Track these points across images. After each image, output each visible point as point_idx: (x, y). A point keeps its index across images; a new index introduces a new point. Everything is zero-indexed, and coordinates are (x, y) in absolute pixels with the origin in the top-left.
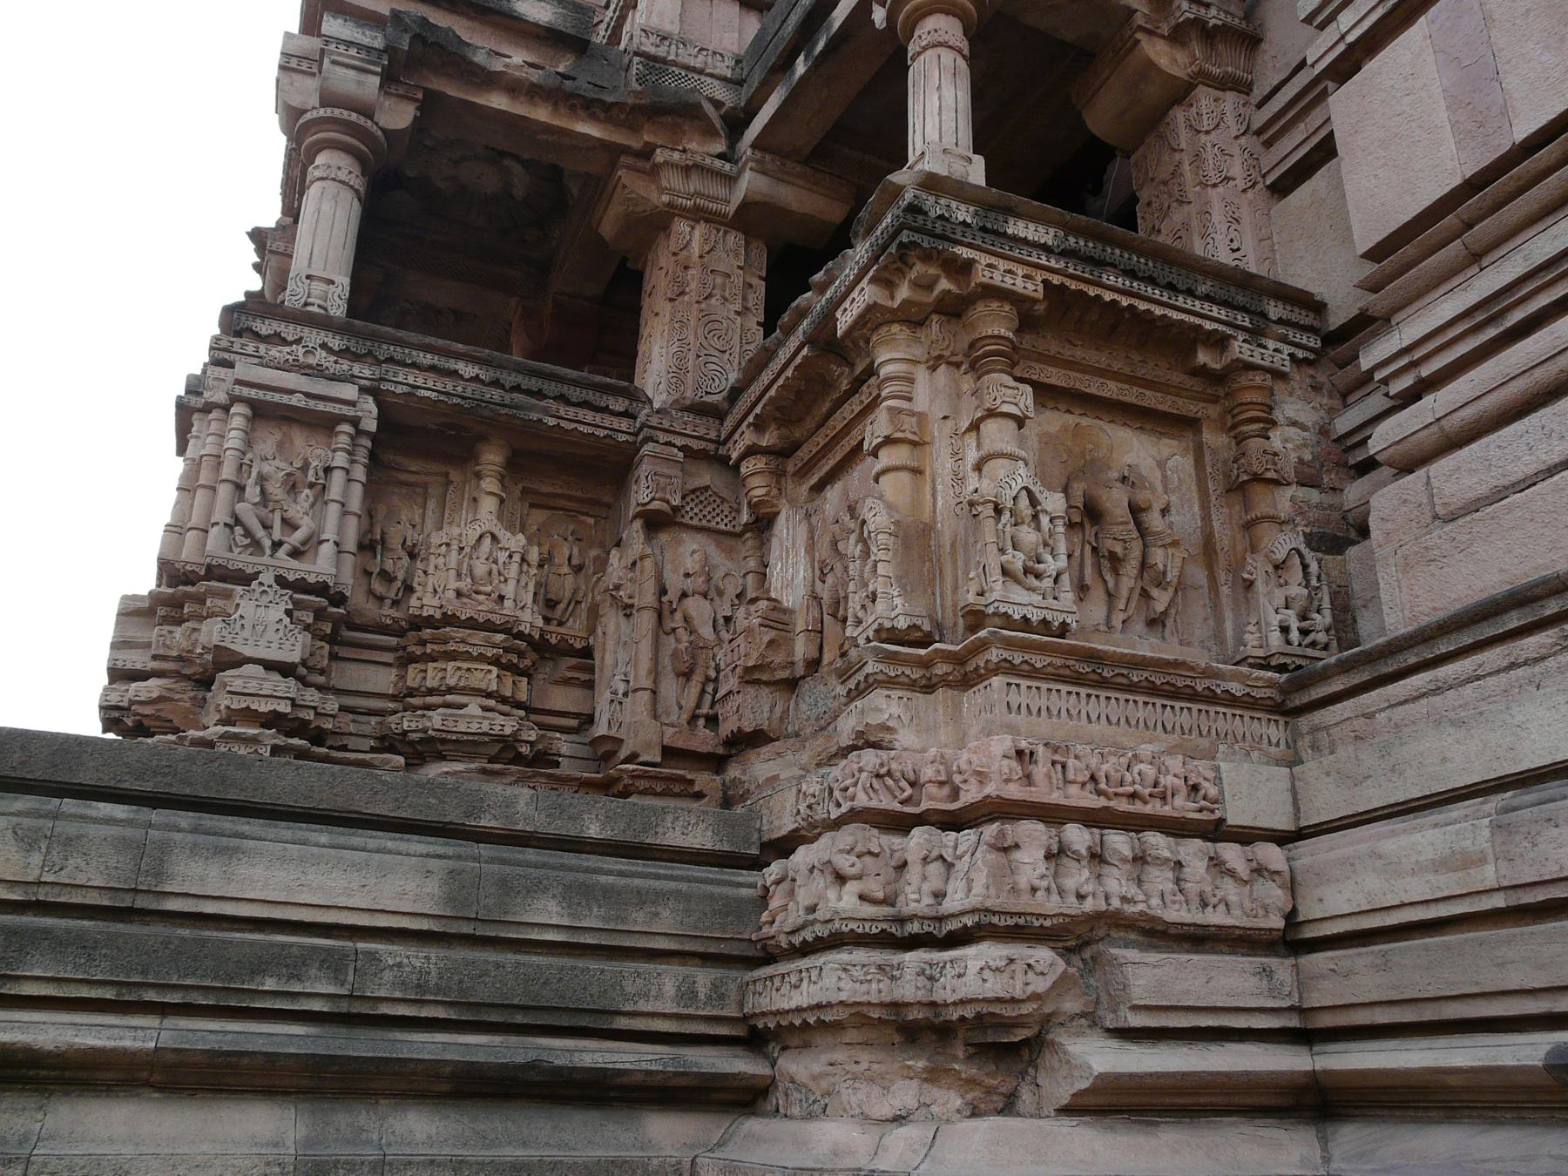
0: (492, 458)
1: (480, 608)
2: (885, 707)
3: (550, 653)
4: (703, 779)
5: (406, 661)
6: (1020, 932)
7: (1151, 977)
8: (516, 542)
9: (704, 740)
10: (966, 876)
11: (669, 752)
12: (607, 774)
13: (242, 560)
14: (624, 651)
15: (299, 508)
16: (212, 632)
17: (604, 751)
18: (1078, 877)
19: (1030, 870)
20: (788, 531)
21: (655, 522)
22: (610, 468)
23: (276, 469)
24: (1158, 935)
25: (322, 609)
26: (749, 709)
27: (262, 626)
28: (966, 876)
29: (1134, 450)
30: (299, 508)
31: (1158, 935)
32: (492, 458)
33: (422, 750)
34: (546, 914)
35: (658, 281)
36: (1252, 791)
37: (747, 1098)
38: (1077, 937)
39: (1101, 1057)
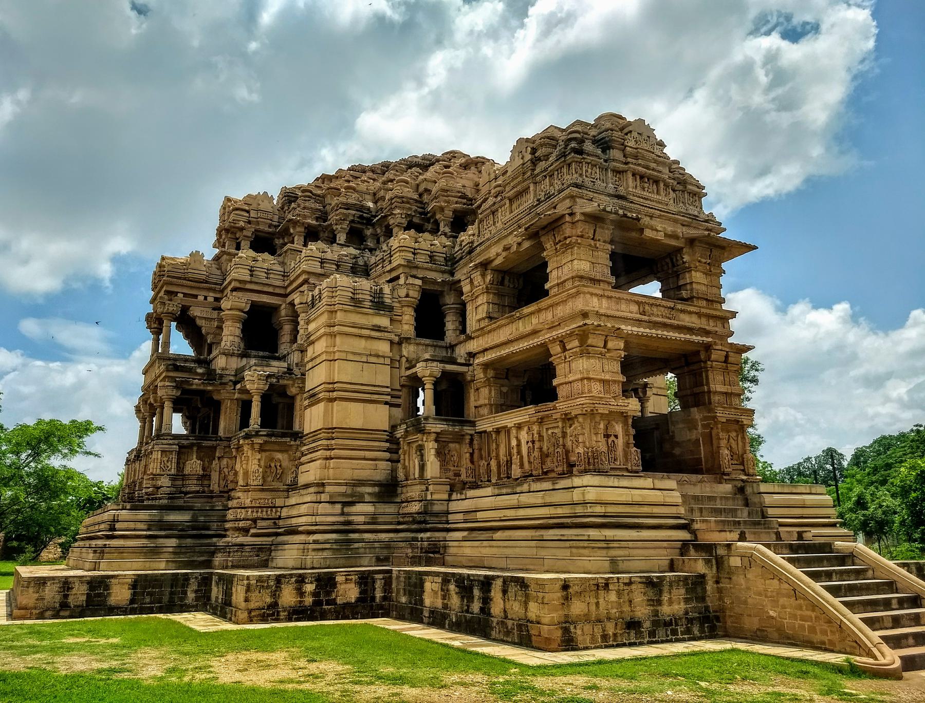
0: (195, 449)
1: (194, 472)
2: (240, 494)
3: (205, 477)
4: (226, 495)
5: (183, 480)
6: (248, 520)
7: (260, 524)
8: (199, 462)
9: (226, 489)
10: (242, 514)
11: (221, 492)
12: (211, 496)
13: (162, 473)
14: (215, 476)
15: (169, 464)
16: (159, 483)
17: (212, 492)
18: (255, 514)
19: (249, 514)
20: (238, 460)
21: (219, 458)
22: (214, 448)
23: (165, 459)
24: (263, 519)
25: (174, 478)
26: (231, 486)
27: (165, 482)
28: (242, 514)
29: (279, 456)
30: (169, 464)
31: (263, 519)
32: (195, 449)
33: (186, 493)
34: (202, 519)
35: (223, 408)
36: (279, 502)
37: (225, 536)
38: (254, 521)
39: (252, 531)
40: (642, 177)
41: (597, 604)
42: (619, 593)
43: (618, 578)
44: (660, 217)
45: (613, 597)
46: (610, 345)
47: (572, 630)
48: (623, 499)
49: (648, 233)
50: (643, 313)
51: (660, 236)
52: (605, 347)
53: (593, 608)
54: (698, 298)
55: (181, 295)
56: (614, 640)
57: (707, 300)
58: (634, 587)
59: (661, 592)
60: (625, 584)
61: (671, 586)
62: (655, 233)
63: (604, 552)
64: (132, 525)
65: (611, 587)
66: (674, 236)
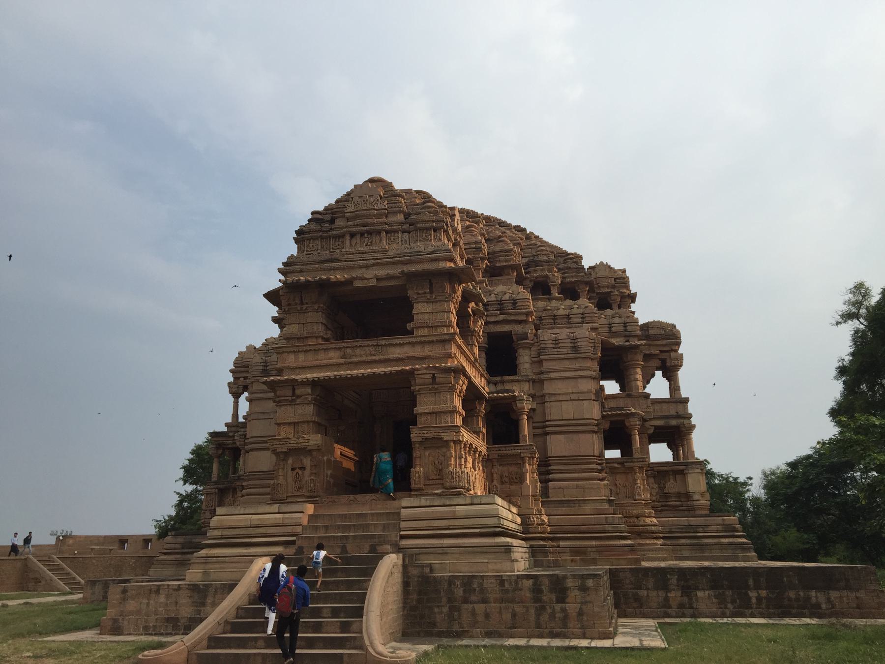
40: (362, 234)
41: (148, 604)
42: (168, 597)
43: (168, 585)
44: (374, 265)
45: (162, 599)
46: (298, 392)
47: (120, 621)
48: (242, 524)
49: (357, 284)
50: (343, 357)
51: (373, 282)
52: (294, 394)
53: (144, 607)
54: (418, 328)
55: (242, 379)
56: (154, 630)
57: (428, 327)
58: (181, 592)
59: (205, 597)
60: (174, 590)
61: (216, 591)
62: (366, 281)
63: (202, 566)
64: (173, 546)
65: (161, 592)
66: (389, 278)
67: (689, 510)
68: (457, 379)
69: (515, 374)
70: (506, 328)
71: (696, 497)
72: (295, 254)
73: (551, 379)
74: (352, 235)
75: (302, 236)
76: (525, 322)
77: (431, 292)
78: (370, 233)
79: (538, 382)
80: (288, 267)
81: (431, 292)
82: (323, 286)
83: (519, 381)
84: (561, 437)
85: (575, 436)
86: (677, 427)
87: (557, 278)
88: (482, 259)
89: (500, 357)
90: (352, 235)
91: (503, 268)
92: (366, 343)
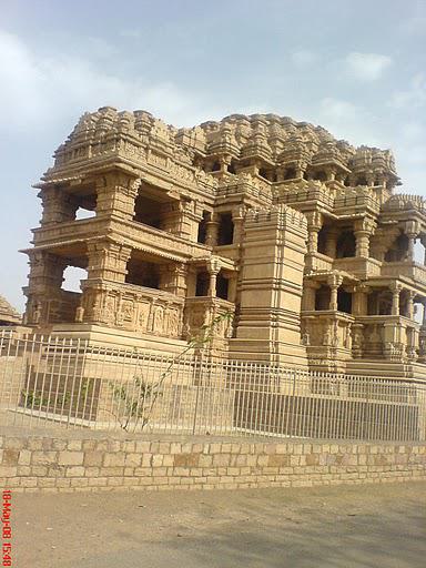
67: (385, 358)
68: (108, 247)
69: (231, 243)
70: (228, 208)
71: (387, 347)
72: (52, 165)
73: (250, 247)
74: (76, 150)
75: (63, 154)
76: (241, 202)
77: (105, 185)
78: (84, 147)
79: (241, 250)
80: (47, 176)
81: (105, 185)
82: (58, 187)
83: (229, 250)
84: (250, 292)
85: (259, 292)
86: (387, 288)
87: (303, 165)
88: (226, 155)
89: (221, 228)
90: (76, 150)
91: (249, 160)
92: (68, 224)
